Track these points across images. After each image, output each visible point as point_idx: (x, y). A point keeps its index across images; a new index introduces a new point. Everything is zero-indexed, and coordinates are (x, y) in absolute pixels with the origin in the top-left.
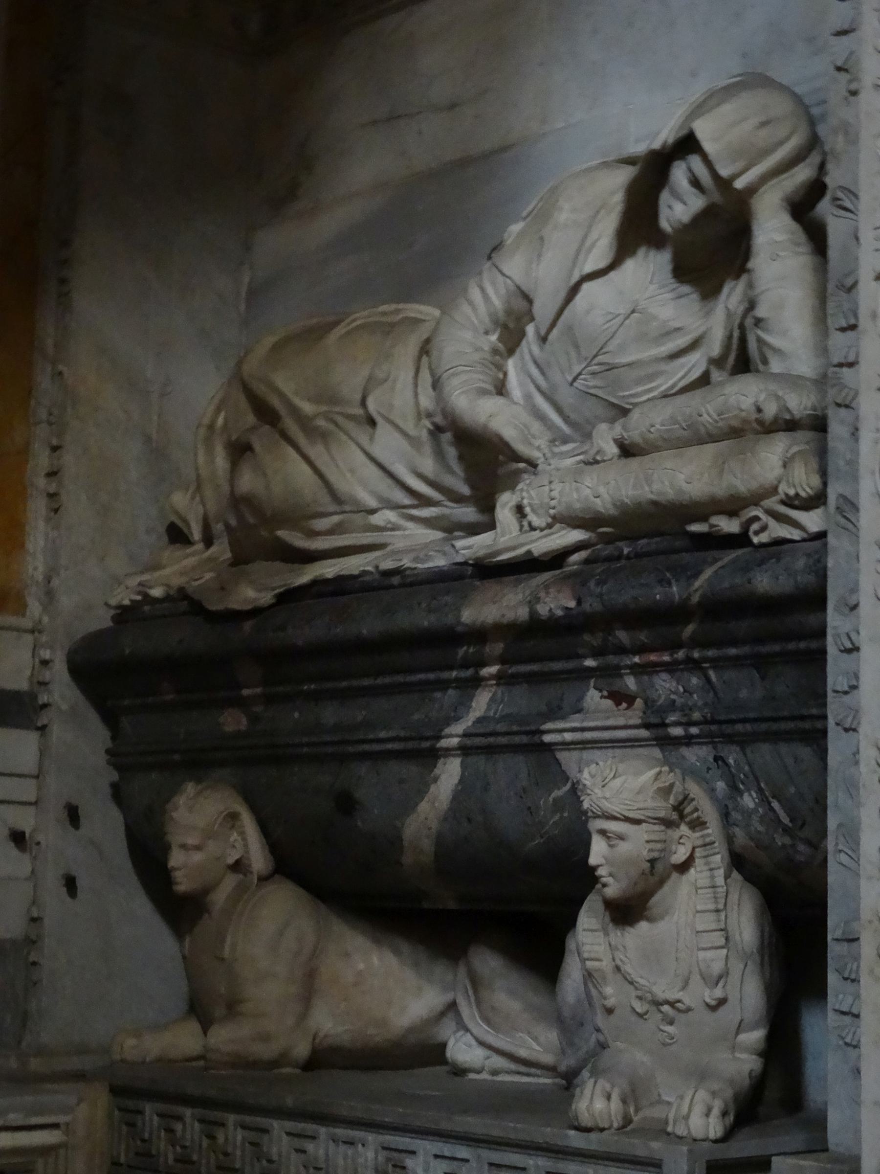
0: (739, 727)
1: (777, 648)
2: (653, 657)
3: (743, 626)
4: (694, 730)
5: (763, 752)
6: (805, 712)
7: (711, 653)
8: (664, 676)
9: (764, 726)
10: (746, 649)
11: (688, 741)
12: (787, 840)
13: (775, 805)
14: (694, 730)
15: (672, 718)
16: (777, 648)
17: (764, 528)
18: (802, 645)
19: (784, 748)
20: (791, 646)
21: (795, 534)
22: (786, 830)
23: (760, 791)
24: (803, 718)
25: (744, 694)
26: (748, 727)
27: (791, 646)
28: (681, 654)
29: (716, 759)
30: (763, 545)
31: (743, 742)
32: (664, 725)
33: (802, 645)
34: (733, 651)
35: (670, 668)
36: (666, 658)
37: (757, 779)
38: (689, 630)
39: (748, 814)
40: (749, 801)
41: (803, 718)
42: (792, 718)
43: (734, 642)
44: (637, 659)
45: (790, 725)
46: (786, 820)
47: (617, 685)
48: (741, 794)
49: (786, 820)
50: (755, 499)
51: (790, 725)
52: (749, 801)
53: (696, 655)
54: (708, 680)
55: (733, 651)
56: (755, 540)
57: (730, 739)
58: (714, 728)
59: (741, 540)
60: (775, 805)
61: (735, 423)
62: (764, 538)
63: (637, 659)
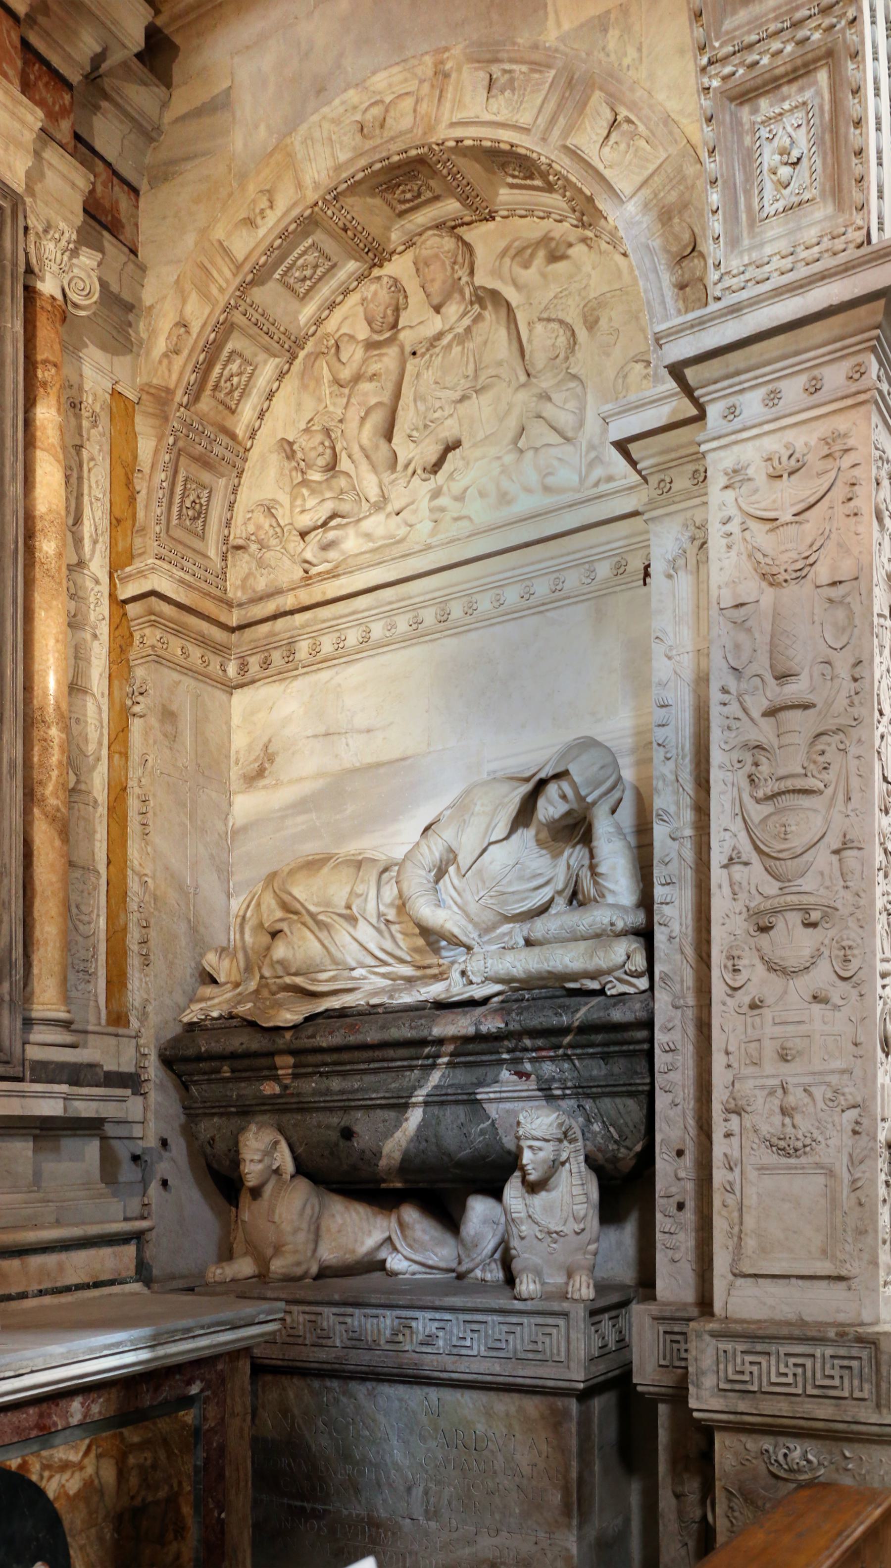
0: (594, 1090)
1: (617, 1048)
2: (544, 1053)
3: (599, 1038)
4: (568, 1092)
5: (607, 1104)
6: (632, 1081)
7: (579, 1051)
8: (549, 1063)
9: (608, 1089)
10: (599, 1049)
11: (564, 1097)
12: (615, 1147)
13: (612, 1129)
14: (568, 1092)
15: (555, 1085)
16: (617, 1048)
17: (614, 987)
18: (631, 1047)
19: (618, 1100)
20: (625, 1048)
21: (632, 990)
22: (616, 1142)
23: (603, 1122)
24: (630, 1085)
25: (595, 1072)
26: (599, 1090)
27: (625, 1048)
28: (561, 1052)
29: (579, 1106)
30: (613, 996)
31: (594, 1097)
32: (550, 1089)
33: (631, 1047)
34: (591, 1050)
35: (552, 1059)
36: (552, 1054)
37: (601, 1116)
38: (567, 1039)
39: (595, 1134)
40: (596, 1127)
41: (630, 1085)
42: (624, 1085)
43: (592, 1045)
44: (534, 1054)
45: (624, 1089)
46: (616, 1136)
47: (520, 1068)
48: (592, 1124)
49: (616, 1136)
50: (609, 972)
51: (624, 1089)
52: (596, 1127)
53: (569, 1052)
54: (574, 1065)
55: (591, 1050)
56: (609, 993)
57: (588, 1096)
58: (580, 1090)
59: (602, 992)
60: (612, 1129)
61: (599, 931)
62: (614, 992)
63: (534, 1054)
